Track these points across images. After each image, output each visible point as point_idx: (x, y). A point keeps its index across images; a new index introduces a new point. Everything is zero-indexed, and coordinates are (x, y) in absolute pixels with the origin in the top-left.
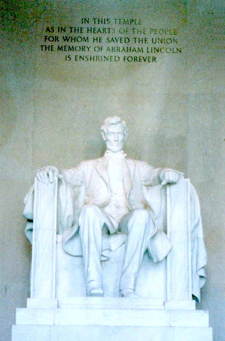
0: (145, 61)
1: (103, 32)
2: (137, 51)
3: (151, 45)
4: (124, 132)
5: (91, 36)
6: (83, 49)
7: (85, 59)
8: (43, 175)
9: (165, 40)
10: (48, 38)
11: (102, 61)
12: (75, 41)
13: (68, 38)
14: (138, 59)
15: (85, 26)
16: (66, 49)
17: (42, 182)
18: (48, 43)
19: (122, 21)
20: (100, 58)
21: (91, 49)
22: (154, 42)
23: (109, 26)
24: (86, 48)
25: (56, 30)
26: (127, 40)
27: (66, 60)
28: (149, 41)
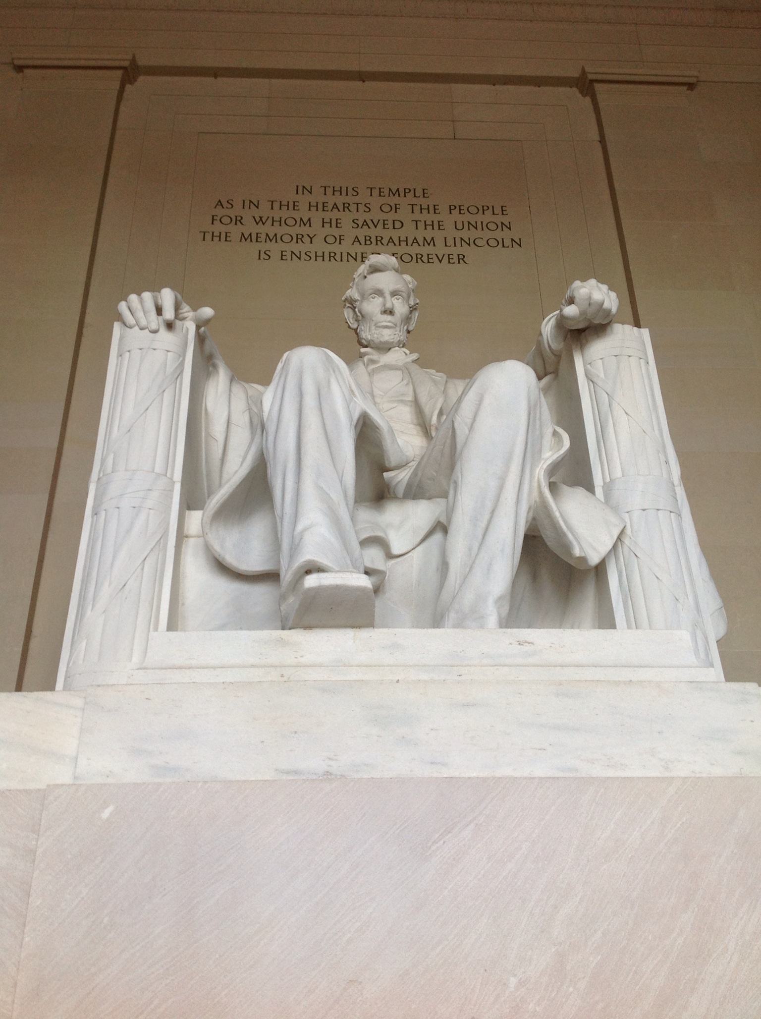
0: (440, 261)
2: (421, 244)
3: (450, 232)
4: (409, 297)
5: (317, 217)
6: (299, 238)
8: (141, 301)
10: (218, 219)
14: (425, 259)
15: (304, 200)
16: (259, 240)
17: (137, 328)
18: (218, 228)
19: (386, 191)
20: (338, 257)
21: (318, 242)
22: (459, 226)
23: (357, 199)
24: (306, 236)
25: (238, 204)
26: (398, 225)
28: (449, 224)
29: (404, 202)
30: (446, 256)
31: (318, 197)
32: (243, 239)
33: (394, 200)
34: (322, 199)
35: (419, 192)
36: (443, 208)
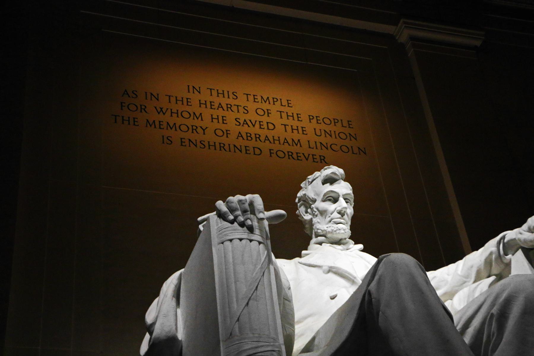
0: (307, 159)
1: (228, 110)
2: (291, 144)
5: (207, 113)
6: (194, 129)
7: (198, 146)
9: (337, 133)
11: (230, 151)
12: (178, 117)
13: (164, 110)
14: (295, 156)
15: (195, 97)
16: (162, 127)
19: (259, 99)
20: (226, 147)
22: (318, 133)
23: (236, 102)
27: (163, 143)
29: (274, 108)
30: (311, 156)
31: (205, 96)
32: (148, 125)
33: (265, 106)
34: (209, 99)
35: (285, 103)
36: (304, 117)
